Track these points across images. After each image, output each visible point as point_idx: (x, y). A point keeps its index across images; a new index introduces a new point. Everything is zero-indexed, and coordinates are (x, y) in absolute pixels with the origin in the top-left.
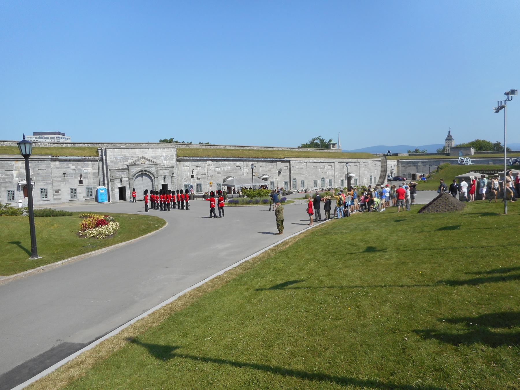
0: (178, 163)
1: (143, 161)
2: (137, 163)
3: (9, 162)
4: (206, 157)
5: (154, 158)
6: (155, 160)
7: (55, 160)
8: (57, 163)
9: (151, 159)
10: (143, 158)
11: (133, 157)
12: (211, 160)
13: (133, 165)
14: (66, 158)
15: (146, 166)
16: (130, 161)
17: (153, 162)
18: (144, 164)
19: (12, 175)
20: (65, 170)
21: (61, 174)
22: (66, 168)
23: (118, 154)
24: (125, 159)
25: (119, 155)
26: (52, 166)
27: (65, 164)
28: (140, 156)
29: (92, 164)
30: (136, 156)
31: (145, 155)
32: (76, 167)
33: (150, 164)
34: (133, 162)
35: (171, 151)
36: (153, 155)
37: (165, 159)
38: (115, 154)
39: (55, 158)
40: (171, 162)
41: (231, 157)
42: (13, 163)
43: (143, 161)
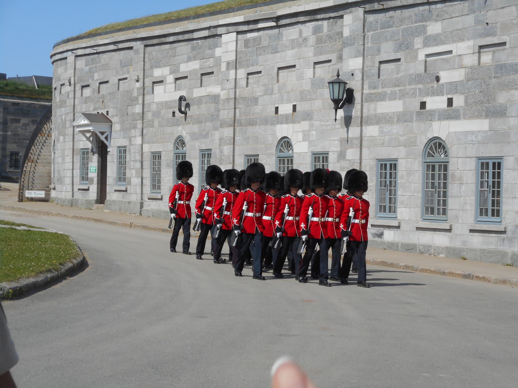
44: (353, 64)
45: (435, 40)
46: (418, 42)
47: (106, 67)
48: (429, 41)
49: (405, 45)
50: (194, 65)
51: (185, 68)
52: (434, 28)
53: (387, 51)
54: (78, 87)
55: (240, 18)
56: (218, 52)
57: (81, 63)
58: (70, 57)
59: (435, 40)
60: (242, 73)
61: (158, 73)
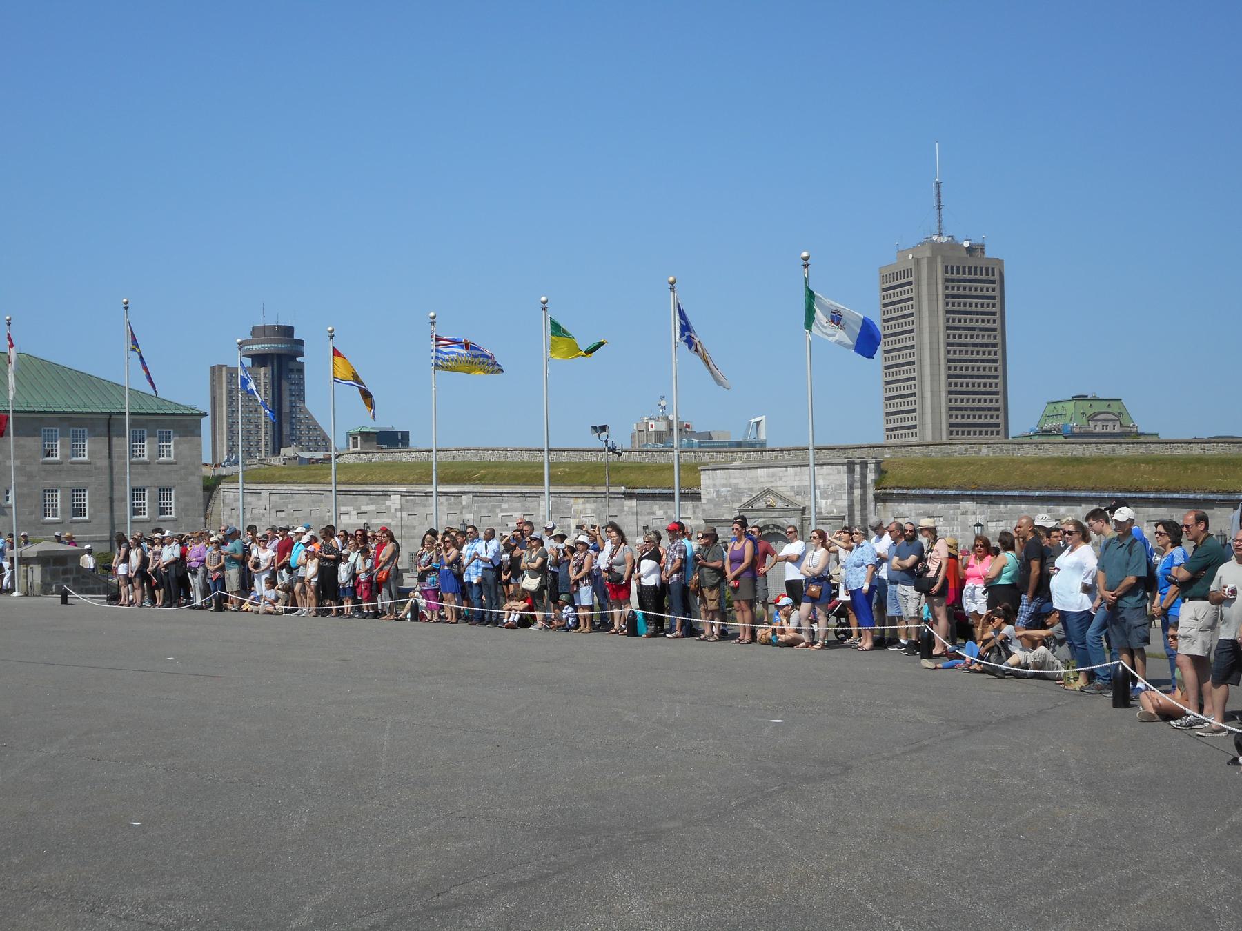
0: (880, 505)
1: (770, 499)
2: (755, 506)
3: (566, 500)
4: (958, 488)
5: (798, 494)
6: (799, 498)
7: (630, 496)
8: (634, 503)
9: (787, 493)
10: (768, 492)
11: (751, 489)
12: (972, 498)
13: (747, 511)
14: (647, 491)
15: (776, 514)
16: (745, 500)
17: (790, 502)
18: (771, 508)
19: (569, 526)
20: (646, 518)
21: (640, 529)
22: (649, 514)
23: (723, 482)
24: (737, 493)
25: (725, 486)
26: (626, 509)
27: (647, 505)
28: (767, 486)
29: (695, 507)
30: (757, 487)
31: (779, 484)
32: (666, 513)
33: (783, 510)
34: (750, 503)
35: (839, 472)
36: (796, 484)
37: (825, 495)
38: (717, 482)
39: (629, 491)
40: (838, 503)
41: (1037, 490)
42: (572, 501)
43: (770, 499)
44: (470, 516)
45: (506, 511)
46: (498, 510)
47: (298, 502)
48: (502, 511)
49: (492, 510)
50: (373, 508)
51: (364, 508)
52: (504, 506)
53: (484, 512)
54: (273, 511)
55: (404, 489)
56: (388, 503)
57: (273, 498)
58: (265, 494)
59: (506, 511)
60: (404, 514)
61: (343, 509)
